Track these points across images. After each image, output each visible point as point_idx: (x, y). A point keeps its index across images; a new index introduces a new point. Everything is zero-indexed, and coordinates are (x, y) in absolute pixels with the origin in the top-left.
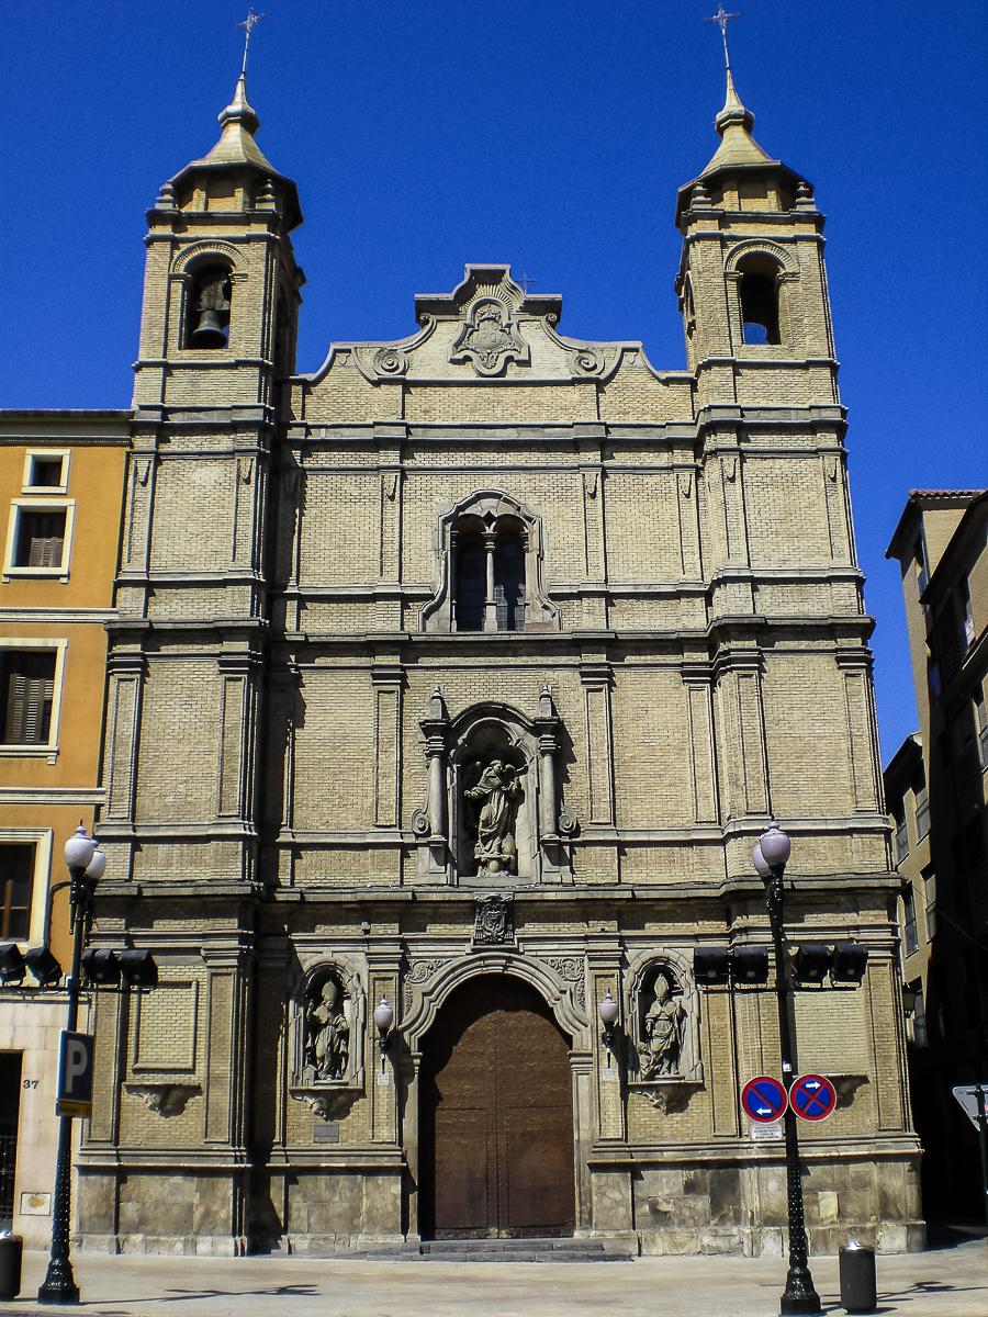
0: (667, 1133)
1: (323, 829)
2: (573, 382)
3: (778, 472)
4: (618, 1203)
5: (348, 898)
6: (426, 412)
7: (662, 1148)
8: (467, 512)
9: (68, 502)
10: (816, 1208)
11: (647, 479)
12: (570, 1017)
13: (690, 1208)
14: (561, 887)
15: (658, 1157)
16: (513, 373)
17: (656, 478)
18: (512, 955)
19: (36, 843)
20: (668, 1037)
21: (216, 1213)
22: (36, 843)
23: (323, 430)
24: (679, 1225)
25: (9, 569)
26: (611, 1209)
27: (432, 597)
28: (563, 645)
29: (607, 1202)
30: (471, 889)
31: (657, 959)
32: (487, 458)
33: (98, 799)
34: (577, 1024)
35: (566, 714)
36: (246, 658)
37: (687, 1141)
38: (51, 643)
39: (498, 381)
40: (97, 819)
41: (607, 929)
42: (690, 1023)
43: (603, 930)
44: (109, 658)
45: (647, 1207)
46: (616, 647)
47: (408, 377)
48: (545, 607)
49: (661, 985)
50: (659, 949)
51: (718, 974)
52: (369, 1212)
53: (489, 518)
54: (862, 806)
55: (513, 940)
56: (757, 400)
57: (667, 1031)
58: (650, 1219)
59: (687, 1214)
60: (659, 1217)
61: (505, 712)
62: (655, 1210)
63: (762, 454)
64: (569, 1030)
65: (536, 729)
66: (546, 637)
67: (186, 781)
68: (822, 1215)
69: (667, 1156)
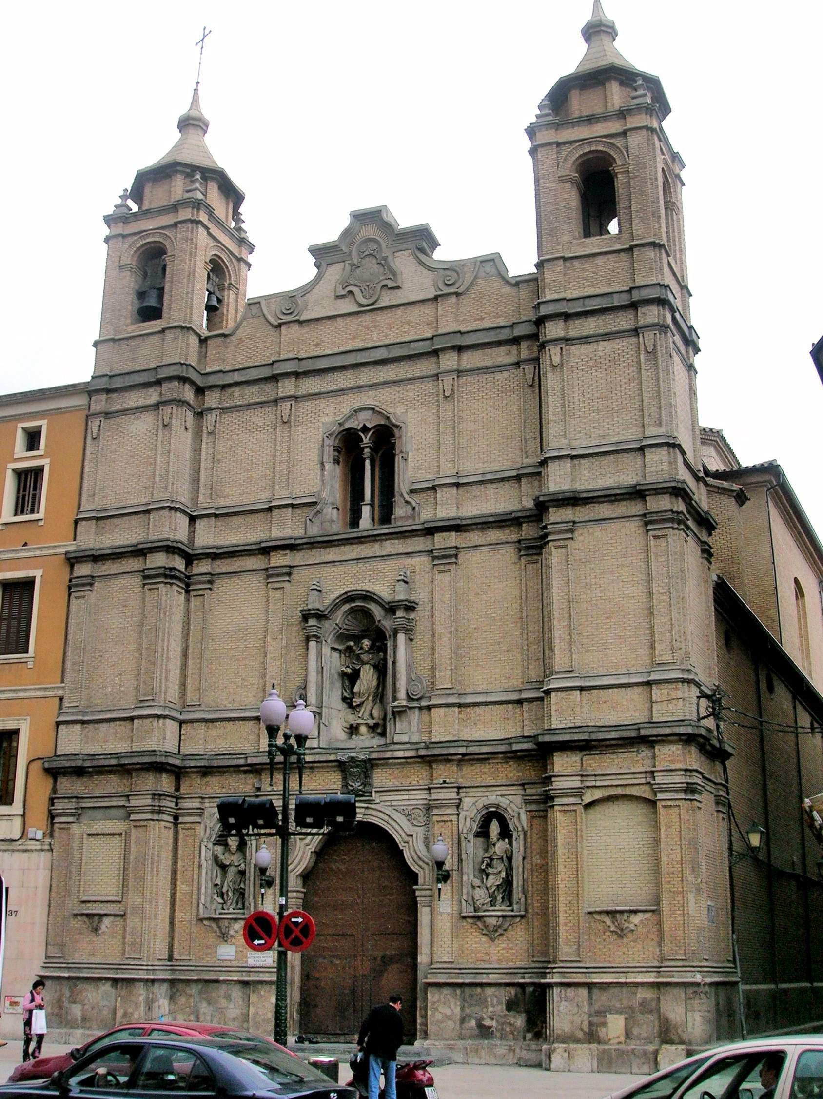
0: (495, 958)
1: (230, 706)
2: (436, 298)
3: (601, 354)
4: (449, 1018)
5: (242, 762)
6: (317, 345)
7: (487, 971)
8: (348, 426)
9: (45, 462)
10: (604, 1030)
11: (498, 376)
12: (416, 858)
13: (510, 1024)
14: (408, 746)
15: (484, 979)
16: (386, 300)
17: (506, 374)
18: (370, 806)
19: (19, 729)
20: (500, 872)
21: (132, 1014)
22: (19, 729)
23: (236, 373)
24: (501, 1038)
25: (8, 515)
26: (442, 1022)
27: (315, 503)
28: (419, 533)
29: (439, 1016)
30: (336, 751)
31: (492, 805)
32: (367, 376)
33: (60, 693)
34: (421, 863)
35: (420, 595)
36: (161, 571)
37: (511, 965)
38: (30, 573)
39: (372, 309)
40: (60, 708)
41: (448, 781)
42: (517, 861)
43: (444, 782)
44: (70, 581)
45: (473, 1023)
46: (458, 527)
47: (302, 318)
48: (407, 502)
49: (495, 828)
50: (493, 798)
51: (344, 819)
52: (254, 1019)
53: (365, 429)
54: (658, 660)
55: (371, 792)
56: (586, 290)
57: (499, 869)
58: (477, 1032)
59: (508, 1029)
60: (484, 1032)
61: (368, 597)
62: (480, 1026)
63: (585, 339)
64: (415, 868)
65: (391, 609)
66: (404, 529)
67: (120, 675)
68: (611, 1036)
69: (492, 978)
